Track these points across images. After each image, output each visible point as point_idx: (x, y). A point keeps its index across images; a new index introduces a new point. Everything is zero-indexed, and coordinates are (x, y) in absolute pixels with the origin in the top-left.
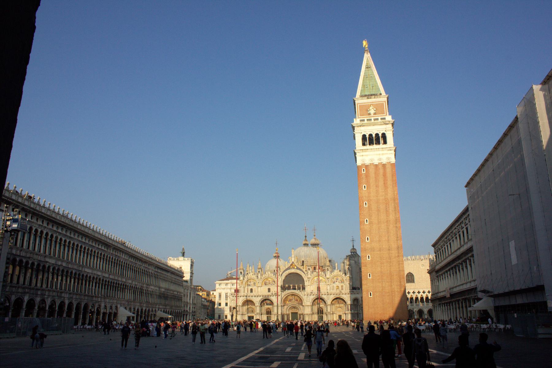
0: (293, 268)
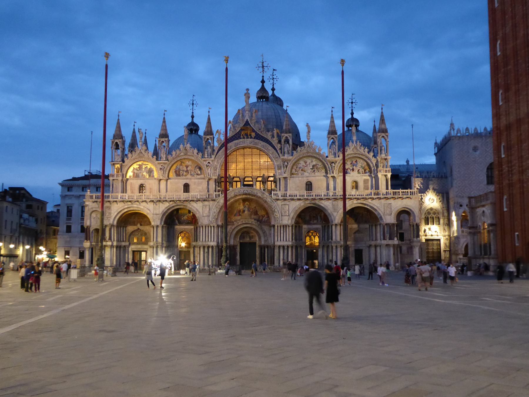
0: (247, 136)
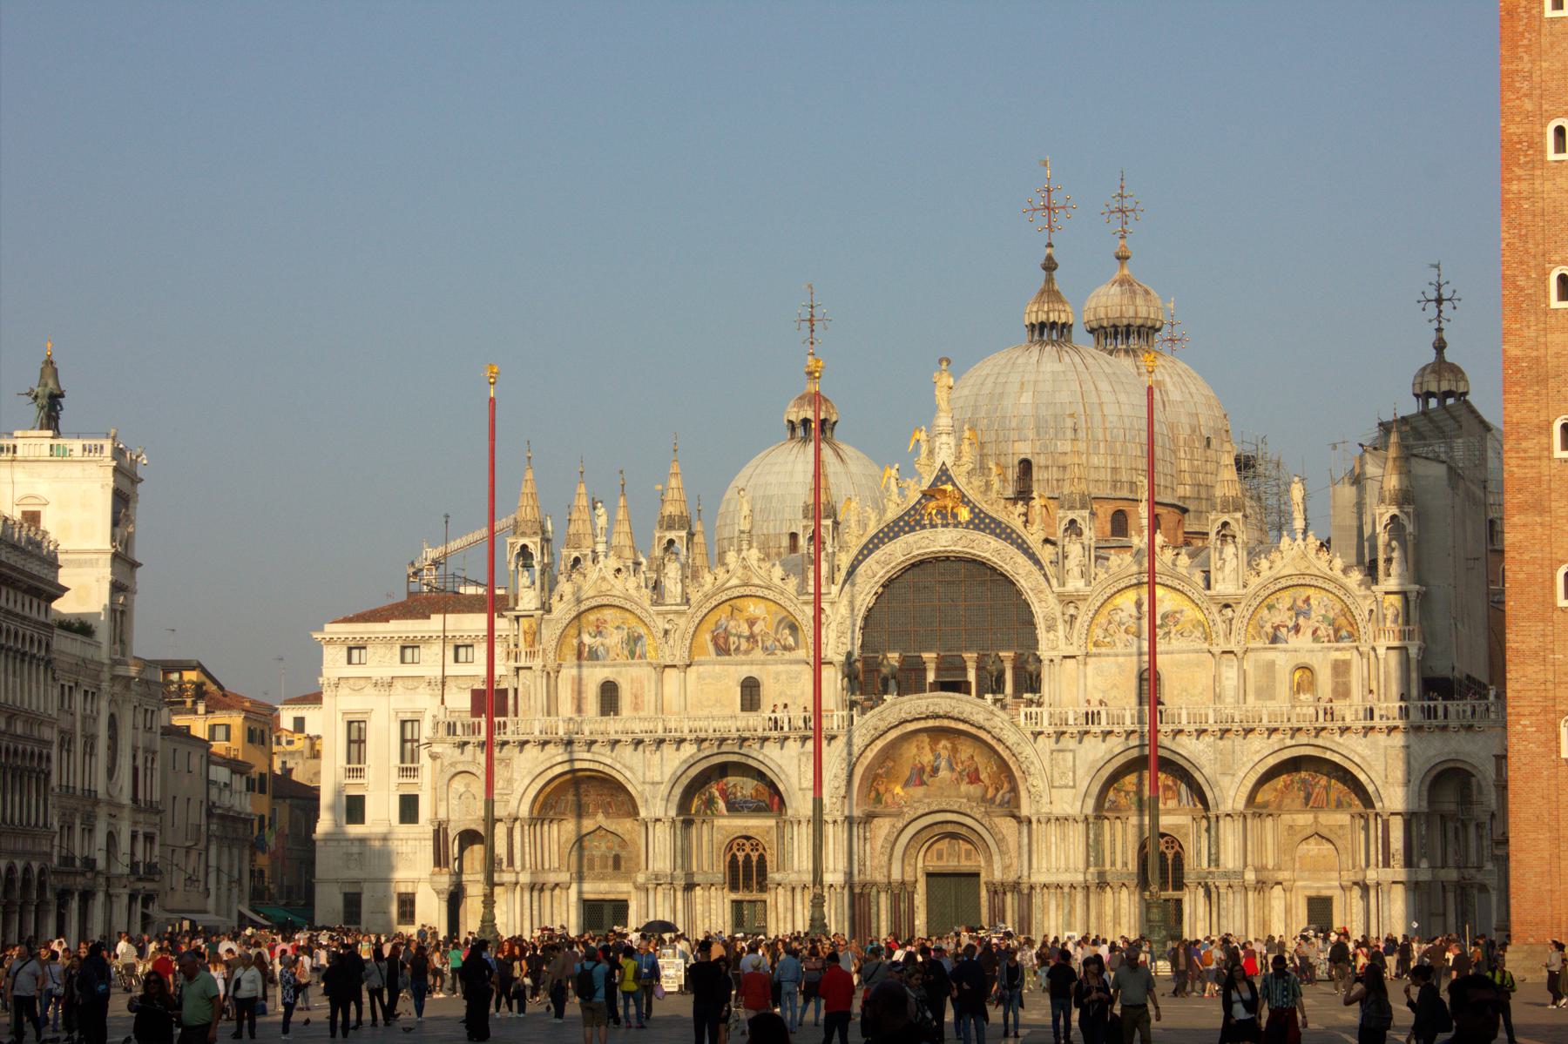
0: (948, 518)
